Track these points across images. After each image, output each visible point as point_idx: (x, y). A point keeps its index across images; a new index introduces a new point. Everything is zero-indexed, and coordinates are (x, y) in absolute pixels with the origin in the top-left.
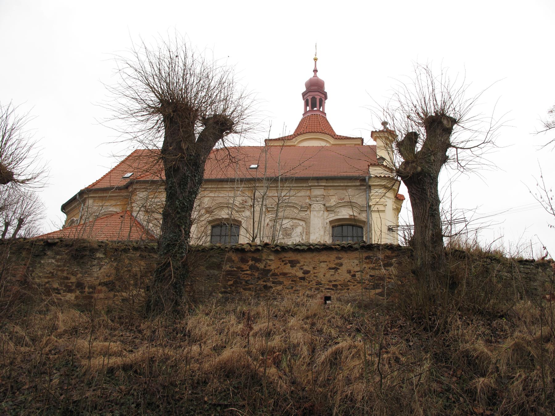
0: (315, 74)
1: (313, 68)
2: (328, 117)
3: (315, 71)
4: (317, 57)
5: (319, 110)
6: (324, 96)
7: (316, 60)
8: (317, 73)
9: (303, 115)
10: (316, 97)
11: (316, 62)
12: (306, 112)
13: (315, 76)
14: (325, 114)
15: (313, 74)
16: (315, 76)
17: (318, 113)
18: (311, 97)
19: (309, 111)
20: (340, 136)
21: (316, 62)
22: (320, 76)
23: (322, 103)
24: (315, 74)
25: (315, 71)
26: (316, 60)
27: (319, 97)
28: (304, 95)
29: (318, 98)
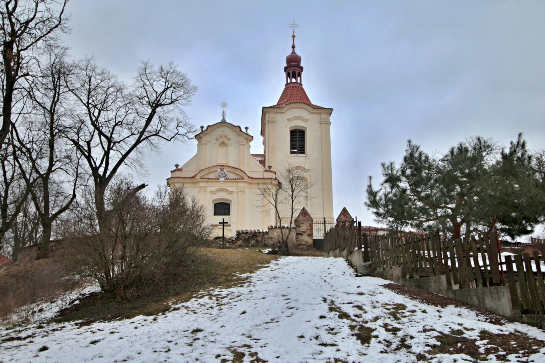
0: (293, 50)
2: (304, 87)
3: (293, 47)
4: (295, 35)
6: (301, 70)
7: (294, 37)
8: (295, 49)
9: (286, 85)
11: (294, 39)
12: (287, 84)
13: (294, 52)
14: (302, 85)
15: (292, 49)
16: (294, 52)
18: (292, 71)
20: (318, 106)
22: (298, 52)
23: (300, 75)
24: (293, 50)
25: (293, 47)
26: (294, 37)
27: (298, 71)
28: (286, 69)
29: (297, 72)
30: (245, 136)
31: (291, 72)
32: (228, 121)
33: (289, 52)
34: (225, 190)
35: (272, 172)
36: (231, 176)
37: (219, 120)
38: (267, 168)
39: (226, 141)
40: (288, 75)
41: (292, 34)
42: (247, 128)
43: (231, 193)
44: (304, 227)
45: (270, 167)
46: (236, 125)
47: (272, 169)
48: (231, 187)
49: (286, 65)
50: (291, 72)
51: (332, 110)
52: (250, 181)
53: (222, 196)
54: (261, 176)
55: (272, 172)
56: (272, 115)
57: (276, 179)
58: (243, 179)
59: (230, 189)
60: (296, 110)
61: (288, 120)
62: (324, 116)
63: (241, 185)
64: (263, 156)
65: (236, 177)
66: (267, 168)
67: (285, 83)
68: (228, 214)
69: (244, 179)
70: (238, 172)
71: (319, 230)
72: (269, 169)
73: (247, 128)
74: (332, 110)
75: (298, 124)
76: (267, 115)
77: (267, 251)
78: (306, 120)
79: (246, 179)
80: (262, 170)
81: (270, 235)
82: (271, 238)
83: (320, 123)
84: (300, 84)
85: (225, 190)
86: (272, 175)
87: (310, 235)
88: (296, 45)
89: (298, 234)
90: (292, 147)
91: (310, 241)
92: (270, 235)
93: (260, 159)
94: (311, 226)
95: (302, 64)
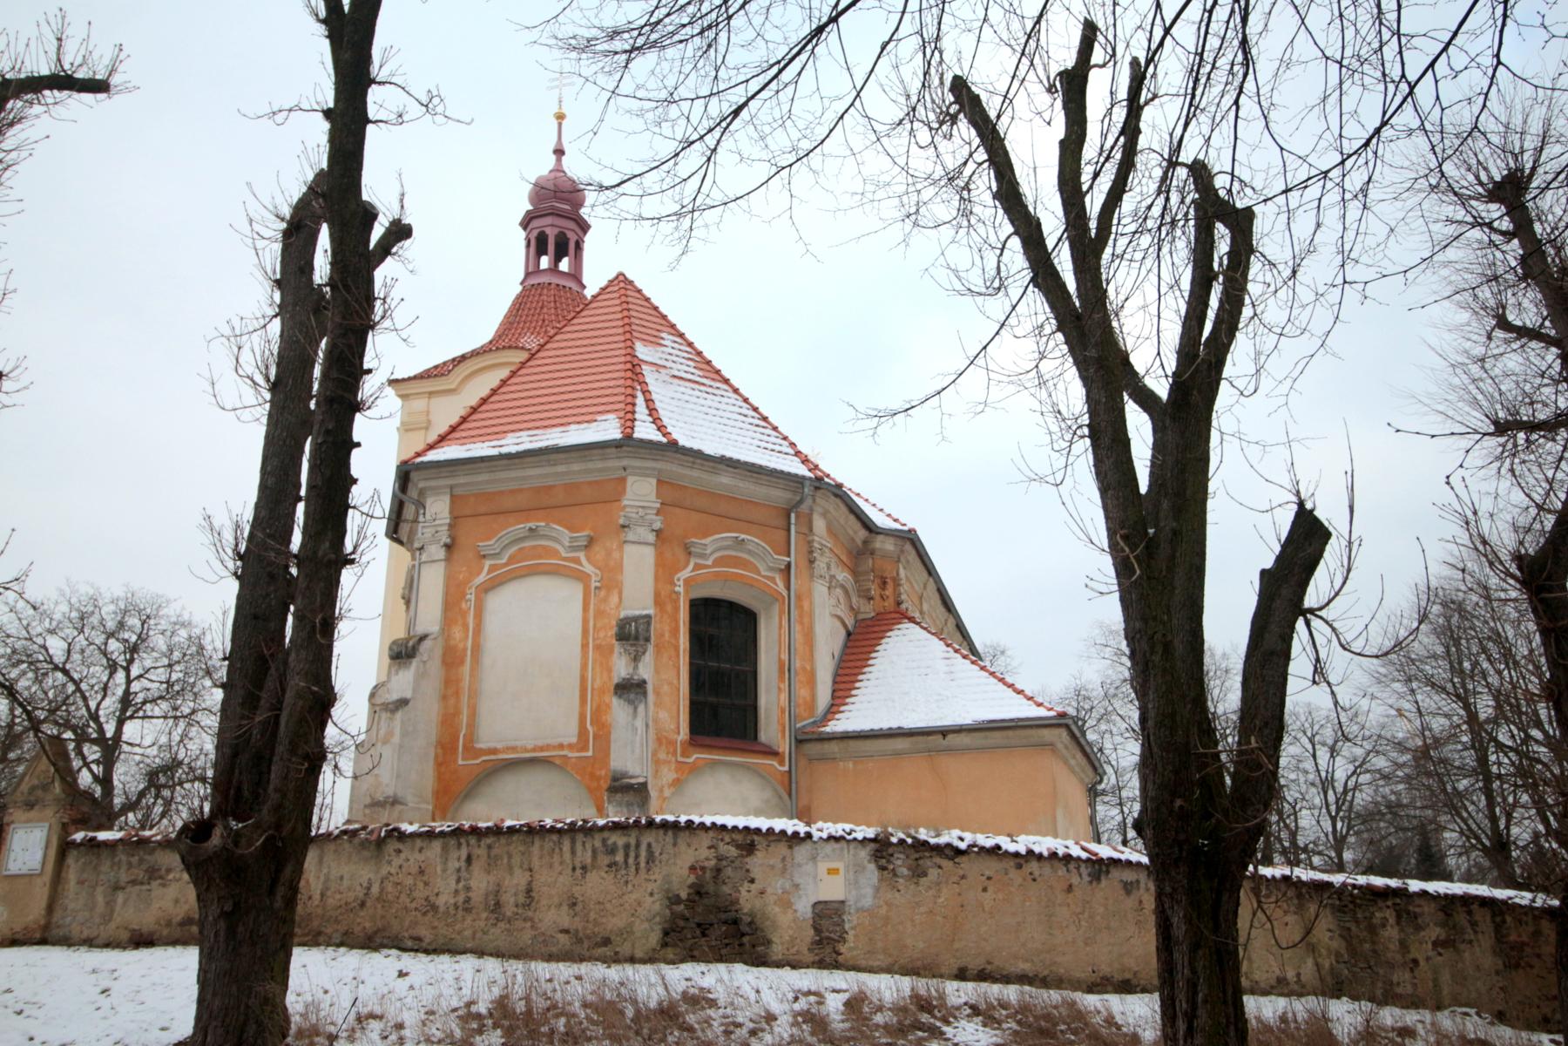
0: (559, 160)
1: (552, 145)
3: (559, 152)
5: (554, 269)
7: (560, 117)
8: (564, 158)
10: (548, 231)
11: (560, 125)
13: (558, 169)
15: (553, 157)
16: (558, 169)
17: (555, 280)
19: (544, 270)
21: (560, 125)
24: (559, 160)
25: (559, 152)
26: (560, 117)
31: (551, 233)
88: (566, 147)
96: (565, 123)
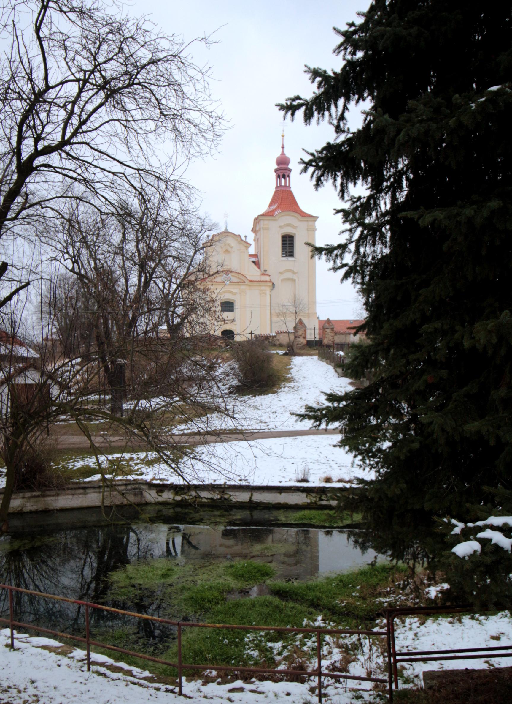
2: (293, 189)
3: (283, 147)
4: (285, 134)
7: (283, 136)
8: (285, 149)
13: (283, 154)
16: (283, 154)
22: (287, 154)
25: (283, 147)
26: (283, 136)
28: (276, 171)
30: (245, 244)
32: (230, 231)
33: (278, 154)
34: (231, 292)
35: (267, 275)
36: (234, 279)
37: (223, 230)
38: (263, 272)
39: (229, 249)
40: (278, 176)
41: (281, 134)
42: (246, 237)
43: (235, 294)
44: (300, 332)
45: (265, 271)
46: (237, 234)
47: (267, 273)
48: (235, 289)
49: (276, 167)
50: (281, 175)
51: (318, 217)
52: (250, 283)
53: (227, 297)
54: (258, 279)
55: (267, 275)
56: (266, 222)
57: (270, 282)
58: (244, 282)
59: (234, 291)
60: (287, 217)
61: (281, 227)
62: (311, 223)
63: (243, 287)
64: (255, 256)
65: (239, 281)
66: (263, 272)
67: (275, 186)
68: (232, 311)
69: (244, 282)
70: (240, 277)
71: (310, 334)
72: (265, 273)
73: (246, 237)
74: (318, 217)
75: (288, 230)
76: (262, 222)
77: (281, 352)
78: (295, 228)
79: (247, 282)
80: (259, 274)
81: (278, 337)
82: (278, 340)
83: (308, 230)
84: (289, 187)
85: (231, 292)
86: (267, 278)
87: (305, 338)
88: (285, 146)
89: (296, 337)
90: (284, 250)
91: (304, 342)
92: (278, 337)
93: (254, 259)
94: (305, 331)
95: (290, 166)
96: (285, 138)
